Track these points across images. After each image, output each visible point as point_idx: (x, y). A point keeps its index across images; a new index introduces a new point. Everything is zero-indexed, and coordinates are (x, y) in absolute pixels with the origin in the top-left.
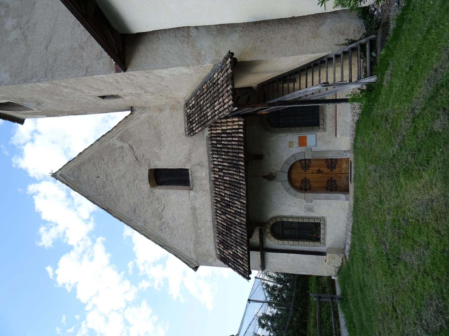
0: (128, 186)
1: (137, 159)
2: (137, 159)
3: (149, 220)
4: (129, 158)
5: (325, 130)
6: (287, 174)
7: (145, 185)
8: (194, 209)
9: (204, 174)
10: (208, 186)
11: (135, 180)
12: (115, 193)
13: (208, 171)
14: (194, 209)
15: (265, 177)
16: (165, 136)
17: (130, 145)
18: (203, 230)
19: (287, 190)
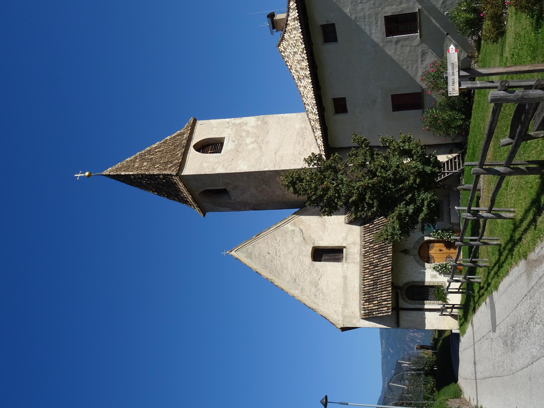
0: (293, 260)
1: (304, 239)
2: (304, 239)
3: (306, 288)
4: (298, 239)
5: (443, 221)
6: (418, 250)
7: (309, 259)
8: (345, 278)
9: (356, 251)
10: (358, 260)
11: (299, 255)
12: (280, 266)
13: (359, 248)
14: (345, 278)
15: (402, 252)
16: (328, 223)
17: (300, 229)
18: (351, 294)
19: (417, 262)
